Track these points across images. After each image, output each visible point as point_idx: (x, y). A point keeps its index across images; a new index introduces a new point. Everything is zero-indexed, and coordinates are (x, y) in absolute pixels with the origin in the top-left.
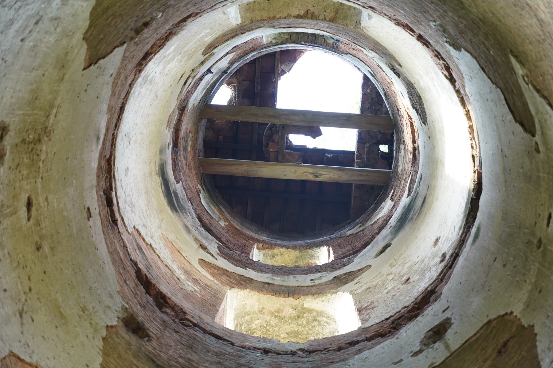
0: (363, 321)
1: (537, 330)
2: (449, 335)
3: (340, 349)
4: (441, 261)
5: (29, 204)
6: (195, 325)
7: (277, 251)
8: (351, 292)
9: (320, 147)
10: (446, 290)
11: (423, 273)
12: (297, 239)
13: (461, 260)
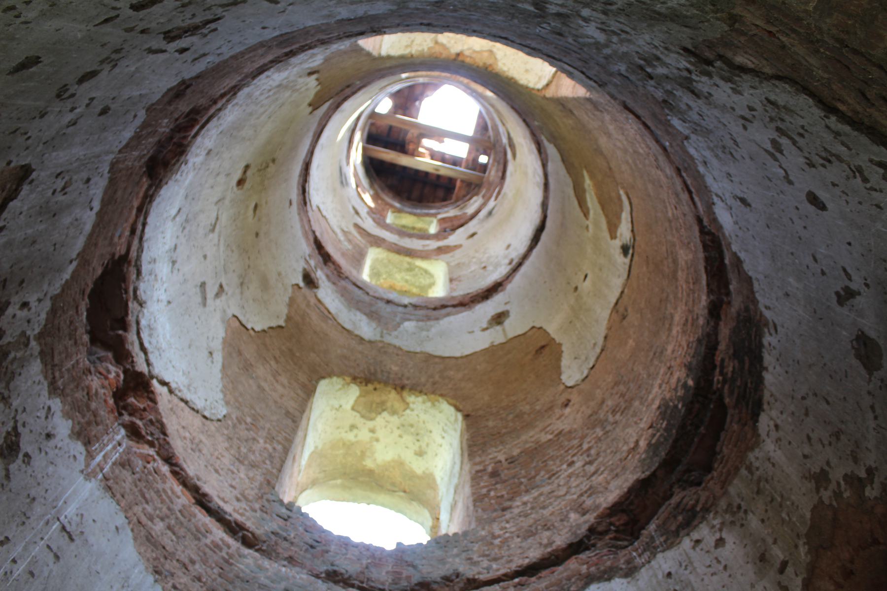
0: (452, 290)
1: (564, 348)
2: (507, 323)
3: (435, 309)
4: (510, 263)
5: (256, 207)
6: (347, 278)
7: (403, 215)
8: (448, 263)
9: (442, 150)
10: (510, 287)
11: (497, 265)
12: (415, 207)
13: (523, 269)
